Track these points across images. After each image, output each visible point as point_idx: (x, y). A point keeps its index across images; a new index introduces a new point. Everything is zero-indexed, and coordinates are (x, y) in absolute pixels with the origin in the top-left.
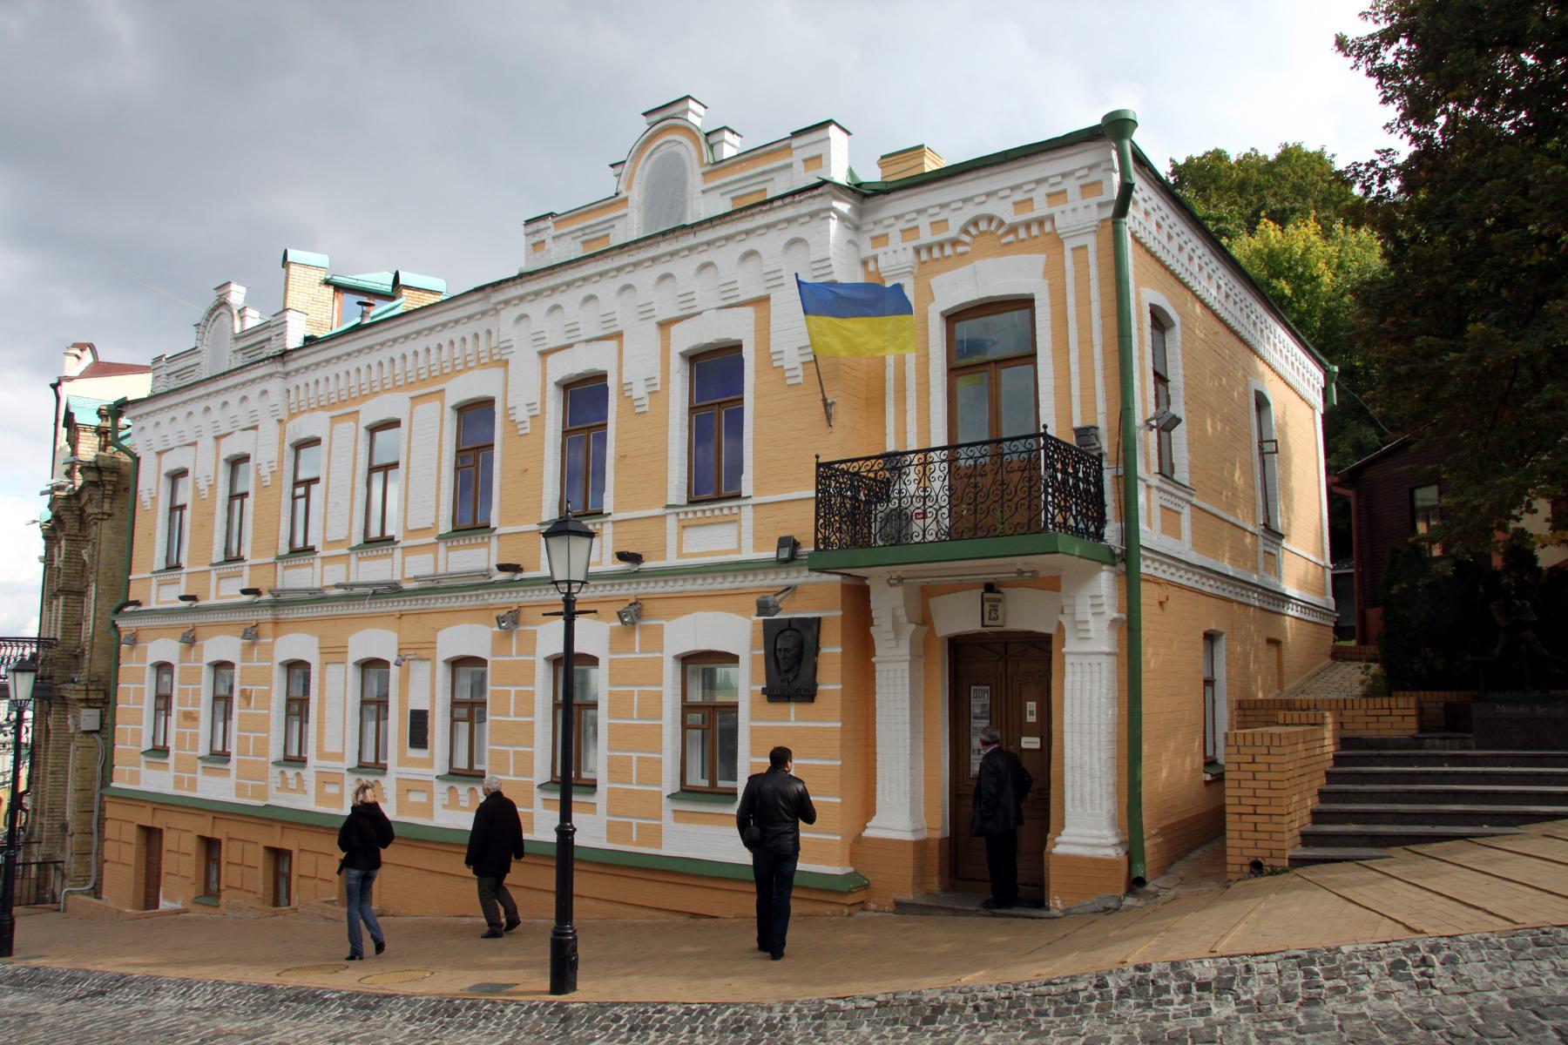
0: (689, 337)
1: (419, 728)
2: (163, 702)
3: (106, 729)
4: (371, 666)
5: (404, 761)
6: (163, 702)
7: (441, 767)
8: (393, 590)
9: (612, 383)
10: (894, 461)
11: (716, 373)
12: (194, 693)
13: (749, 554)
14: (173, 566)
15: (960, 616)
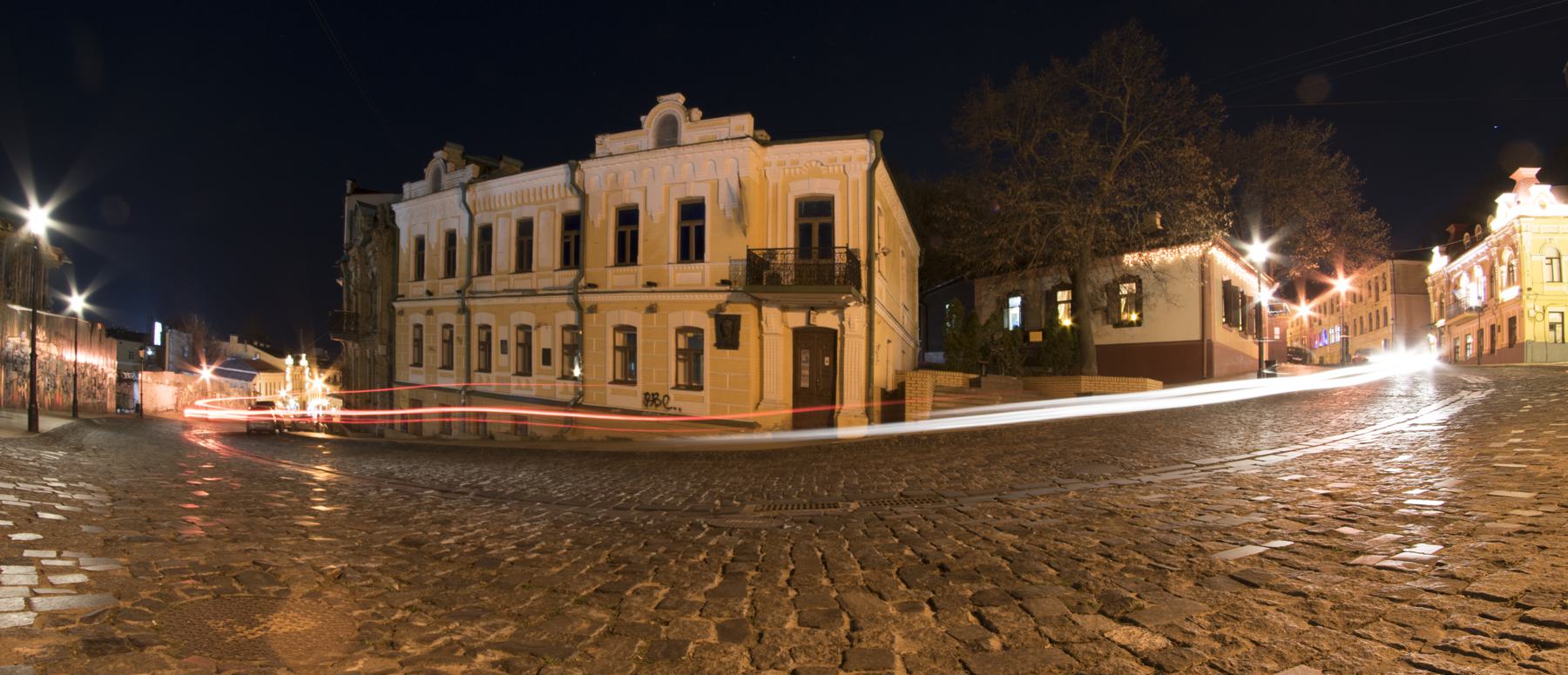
0: (679, 194)
1: (547, 356)
2: (418, 343)
3: (391, 352)
4: (525, 329)
5: (540, 372)
6: (418, 343)
7: (558, 374)
8: (533, 293)
9: (641, 209)
10: (772, 253)
11: (692, 211)
12: (433, 340)
13: (707, 286)
14: (420, 275)
15: (798, 319)
